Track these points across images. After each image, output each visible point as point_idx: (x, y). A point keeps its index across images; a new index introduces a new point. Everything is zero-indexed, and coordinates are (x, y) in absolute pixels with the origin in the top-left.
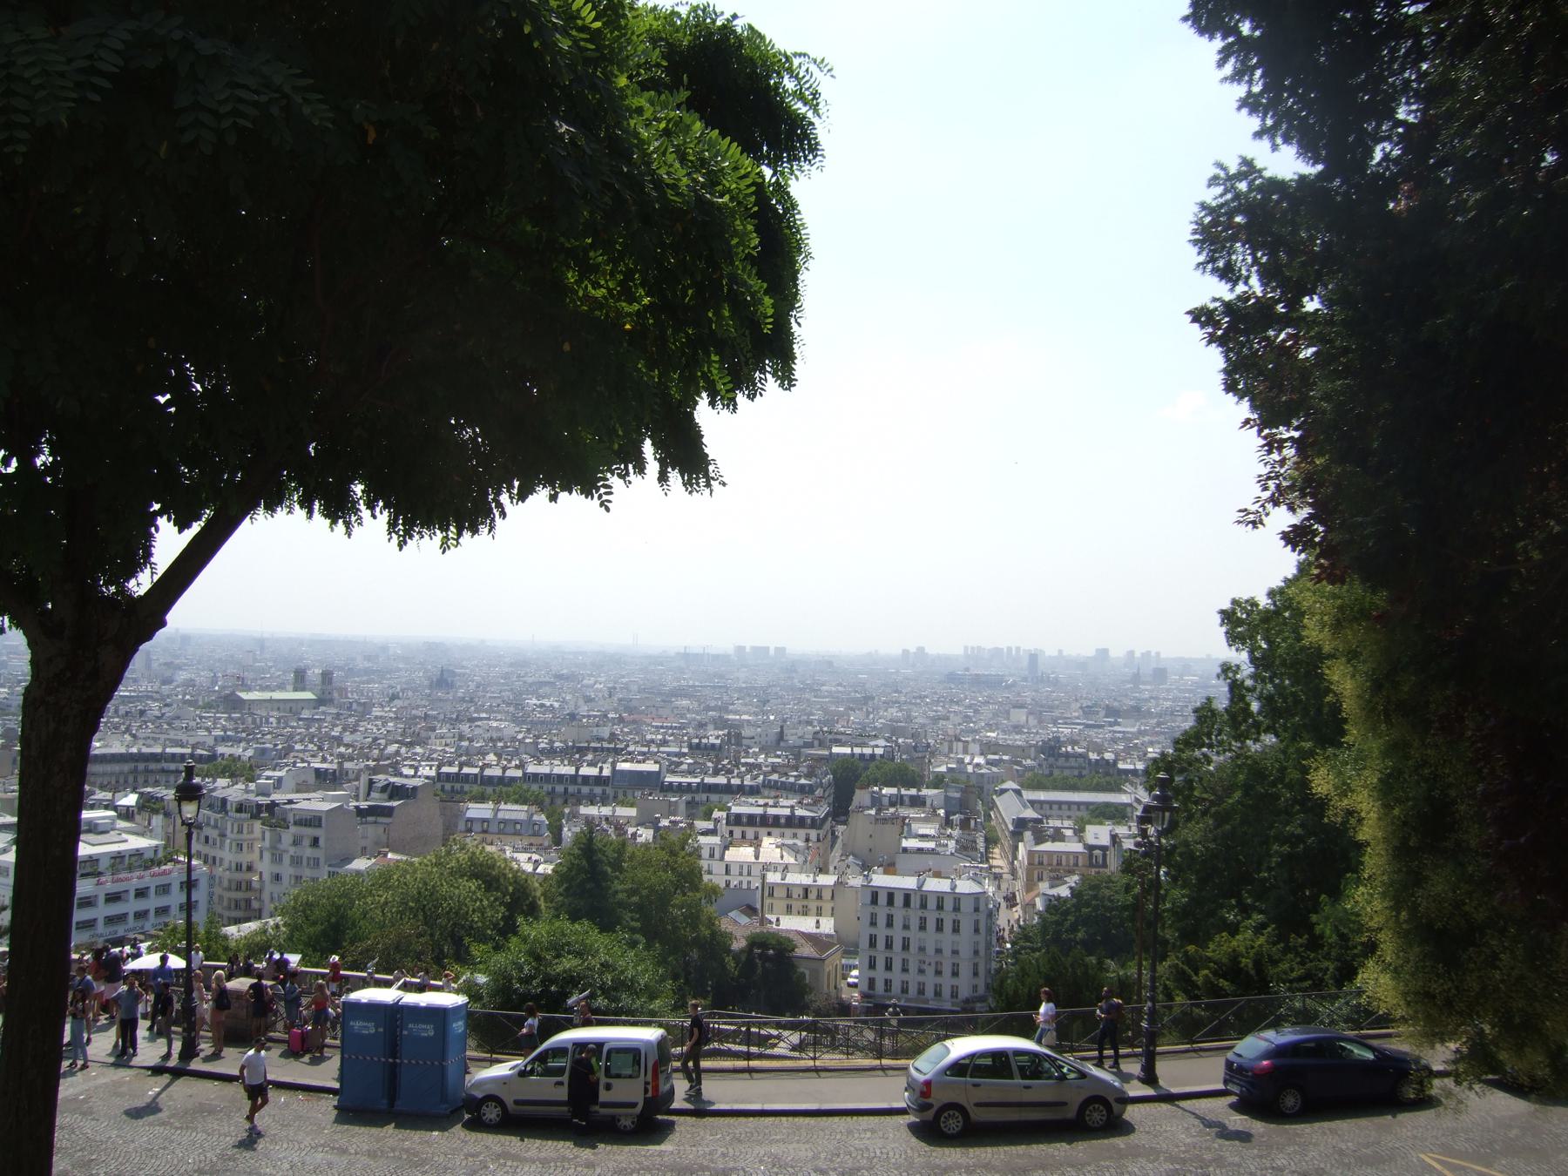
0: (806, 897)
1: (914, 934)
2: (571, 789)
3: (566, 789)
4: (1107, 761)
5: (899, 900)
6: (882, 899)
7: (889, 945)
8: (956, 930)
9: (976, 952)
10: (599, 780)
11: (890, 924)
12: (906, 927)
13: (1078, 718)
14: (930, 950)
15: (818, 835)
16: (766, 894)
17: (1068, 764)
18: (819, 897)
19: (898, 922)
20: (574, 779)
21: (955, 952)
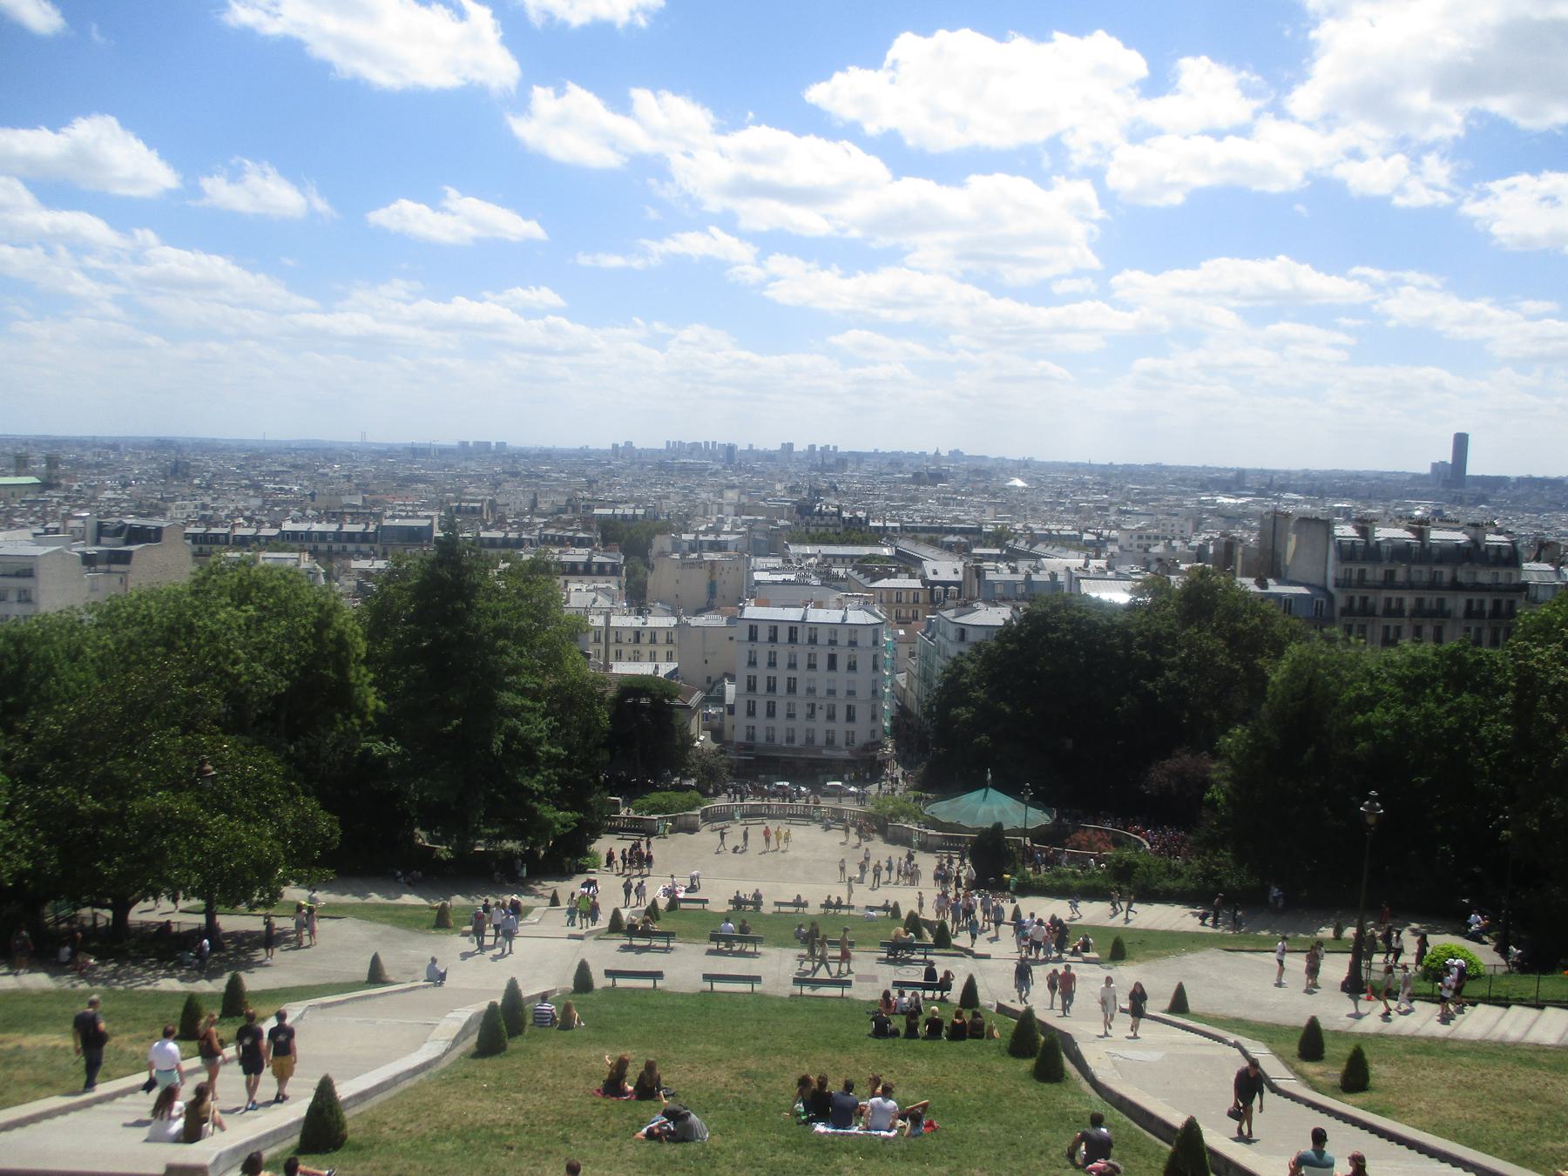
0: (637, 640)
1: (801, 674)
2: (335, 547)
3: (330, 548)
5: (783, 635)
6: (763, 634)
7: (771, 688)
10: (364, 537)
12: (792, 666)
14: (821, 691)
16: (612, 639)
17: (823, 522)
18: (653, 641)
19: (782, 661)
20: (338, 536)
21: (851, 693)
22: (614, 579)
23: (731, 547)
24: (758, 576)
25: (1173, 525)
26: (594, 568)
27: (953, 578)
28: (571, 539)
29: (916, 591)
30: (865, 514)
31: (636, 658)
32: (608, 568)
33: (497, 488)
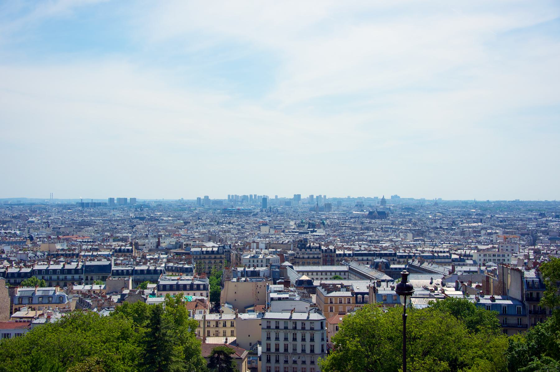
0: (217, 326)
2: (61, 277)
3: (58, 278)
4: (331, 250)
8: (312, 340)
9: (323, 351)
10: (76, 271)
11: (277, 339)
13: (294, 229)
15: (207, 293)
22: (204, 293)
23: (261, 274)
24: (273, 295)
25: (507, 247)
26: (195, 286)
27: (367, 291)
28: (181, 268)
29: (349, 298)
30: (333, 247)
31: (217, 335)
32: (202, 287)
33: (133, 228)
